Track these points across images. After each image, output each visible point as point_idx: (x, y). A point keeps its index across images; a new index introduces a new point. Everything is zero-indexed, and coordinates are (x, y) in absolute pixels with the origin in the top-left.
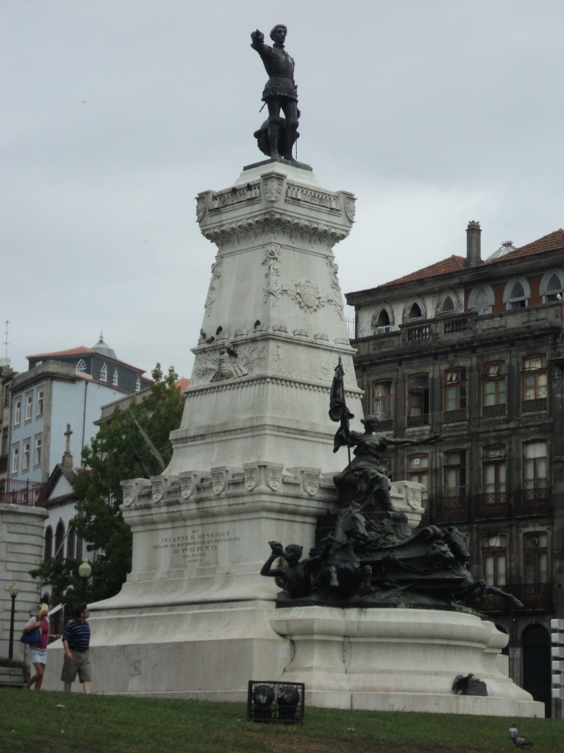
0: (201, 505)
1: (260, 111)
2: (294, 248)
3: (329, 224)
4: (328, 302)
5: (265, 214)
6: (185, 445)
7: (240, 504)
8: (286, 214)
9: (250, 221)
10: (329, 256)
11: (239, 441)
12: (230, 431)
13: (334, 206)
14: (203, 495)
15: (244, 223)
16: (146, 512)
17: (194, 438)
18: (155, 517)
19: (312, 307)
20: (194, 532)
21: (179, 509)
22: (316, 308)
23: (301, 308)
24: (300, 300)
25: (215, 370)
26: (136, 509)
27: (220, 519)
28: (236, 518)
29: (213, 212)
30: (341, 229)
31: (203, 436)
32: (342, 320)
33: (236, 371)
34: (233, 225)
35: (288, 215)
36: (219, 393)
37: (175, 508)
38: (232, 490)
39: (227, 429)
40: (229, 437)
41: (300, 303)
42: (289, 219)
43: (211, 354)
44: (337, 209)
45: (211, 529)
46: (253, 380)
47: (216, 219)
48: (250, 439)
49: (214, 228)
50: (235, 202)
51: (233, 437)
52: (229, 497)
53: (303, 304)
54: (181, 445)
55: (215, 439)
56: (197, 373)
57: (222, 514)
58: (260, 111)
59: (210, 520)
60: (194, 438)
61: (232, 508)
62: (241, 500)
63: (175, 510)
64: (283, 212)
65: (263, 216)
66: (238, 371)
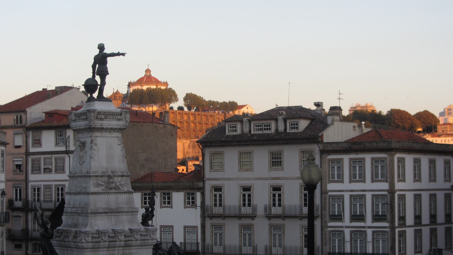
0: (127, 243)
5: (124, 126)
6: (96, 215)
7: (146, 243)
9: (116, 127)
11: (125, 216)
12: (121, 212)
14: (128, 239)
15: (114, 127)
16: (97, 244)
17: (102, 213)
18: (101, 246)
20: (118, 252)
21: (115, 244)
25: (104, 185)
26: (92, 243)
27: (132, 248)
28: (140, 247)
29: (99, 119)
31: (106, 213)
33: (117, 187)
34: (108, 127)
36: (108, 195)
37: (113, 243)
38: (143, 238)
39: (120, 211)
40: (120, 214)
43: (100, 178)
45: (127, 251)
46: (126, 192)
47: (100, 122)
48: (129, 216)
49: (98, 125)
50: (111, 118)
51: (122, 214)
52: (141, 240)
54: (94, 215)
55: (112, 214)
56: (94, 185)
57: (135, 246)
59: (128, 248)
60: (102, 213)
61: (142, 244)
62: (147, 241)
63: (113, 244)
65: (123, 126)
66: (118, 187)
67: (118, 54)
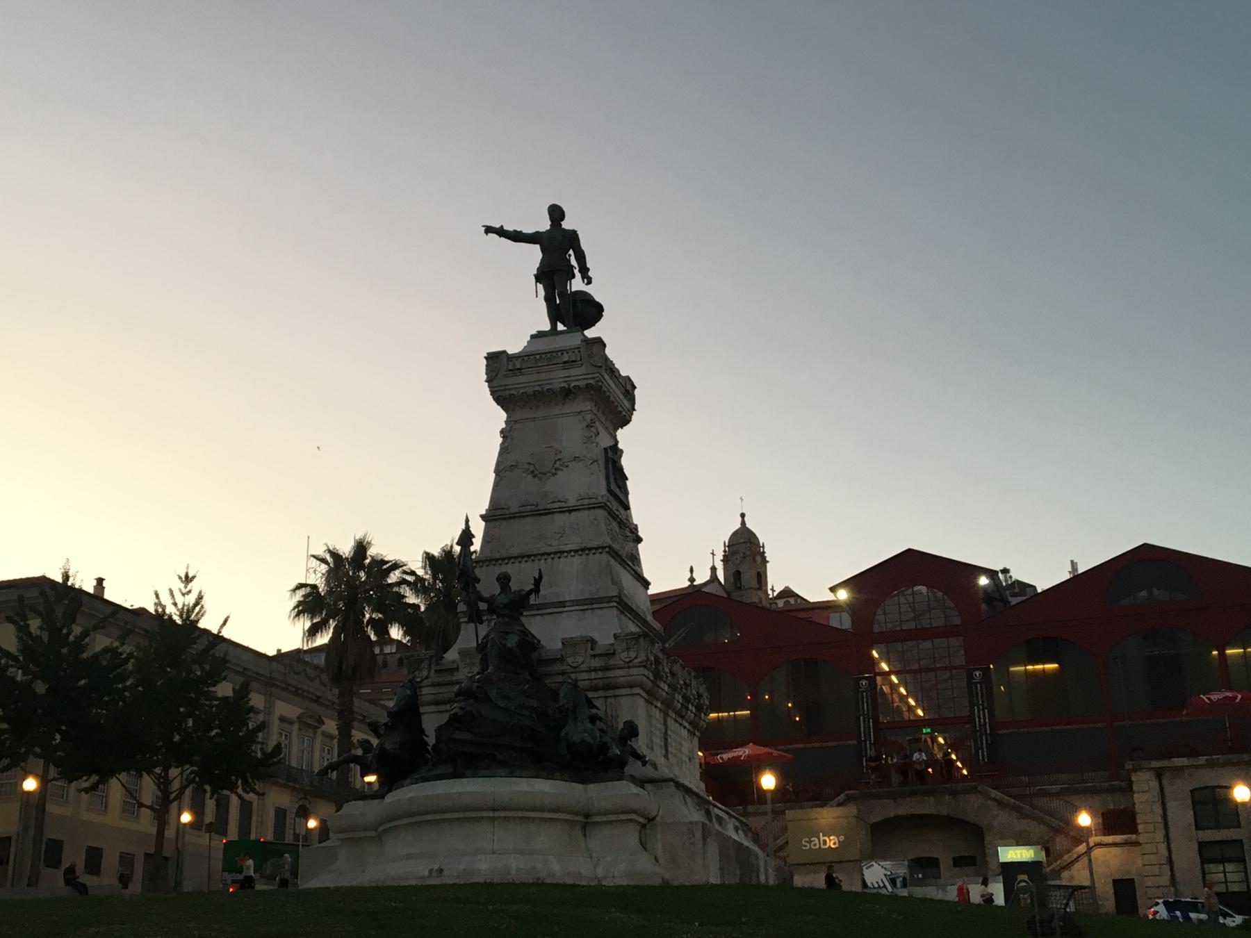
1: (537, 296)
2: (535, 418)
3: (567, 379)
4: (574, 460)
8: (507, 389)
10: (582, 412)
13: (566, 359)
19: (548, 472)
22: (554, 471)
23: (534, 477)
24: (532, 468)
30: (584, 379)
32: (592, 474)
35: (512, 389)
41: (532, 472)
42: (512, 392)
44: (571, 360)
53: (536, 472)
58: (537, 296)
64: (503, 388)
67: (501, 232)
